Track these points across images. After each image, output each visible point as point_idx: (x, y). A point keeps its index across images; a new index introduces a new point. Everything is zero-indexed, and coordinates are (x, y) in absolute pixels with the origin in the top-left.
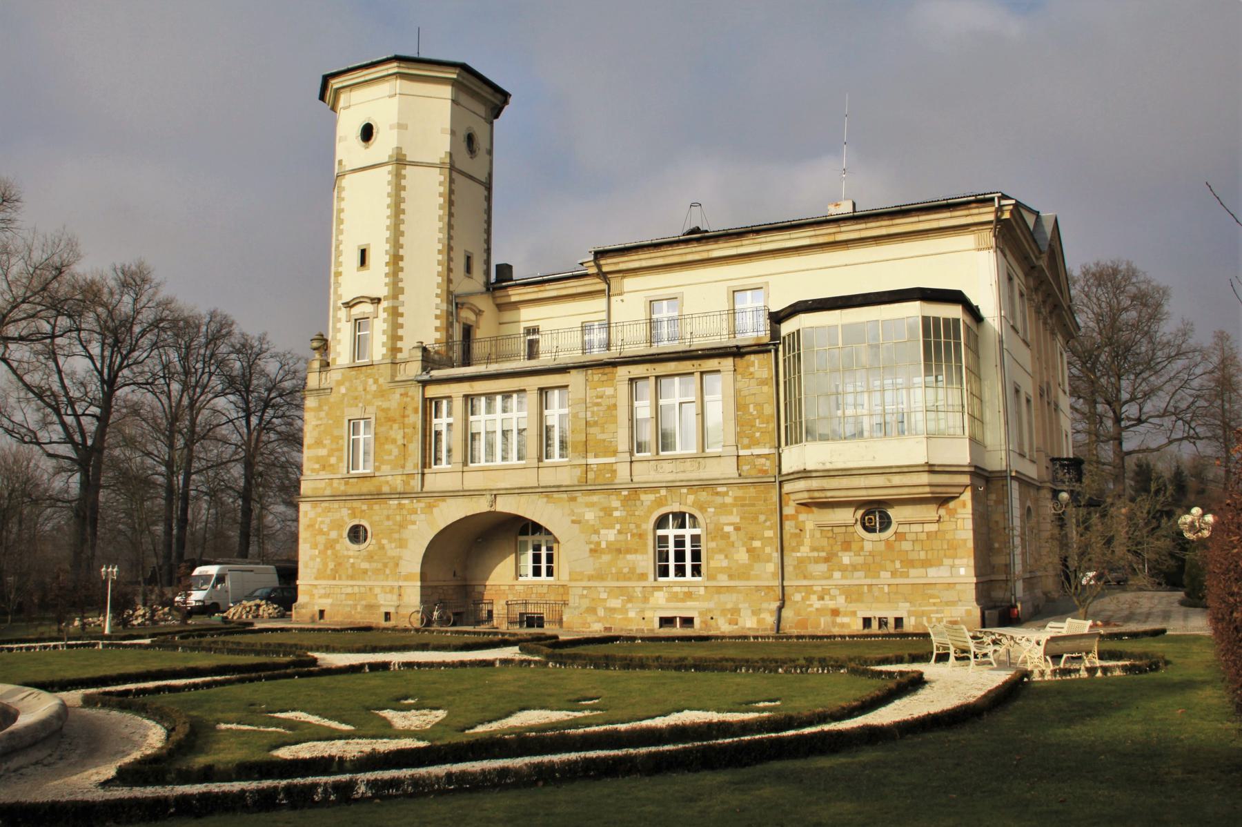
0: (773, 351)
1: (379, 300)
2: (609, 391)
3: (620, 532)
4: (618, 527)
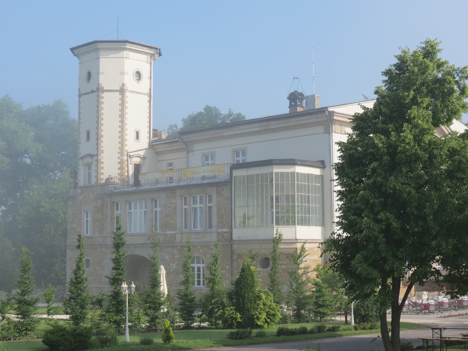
0: (229, 185)
1: (94, 155)
2: (174, 201)
3: (177, 265)
4: (176, 262)
